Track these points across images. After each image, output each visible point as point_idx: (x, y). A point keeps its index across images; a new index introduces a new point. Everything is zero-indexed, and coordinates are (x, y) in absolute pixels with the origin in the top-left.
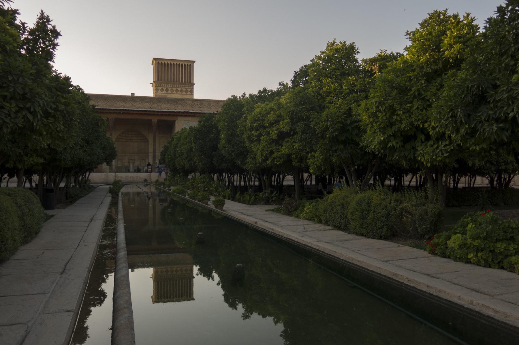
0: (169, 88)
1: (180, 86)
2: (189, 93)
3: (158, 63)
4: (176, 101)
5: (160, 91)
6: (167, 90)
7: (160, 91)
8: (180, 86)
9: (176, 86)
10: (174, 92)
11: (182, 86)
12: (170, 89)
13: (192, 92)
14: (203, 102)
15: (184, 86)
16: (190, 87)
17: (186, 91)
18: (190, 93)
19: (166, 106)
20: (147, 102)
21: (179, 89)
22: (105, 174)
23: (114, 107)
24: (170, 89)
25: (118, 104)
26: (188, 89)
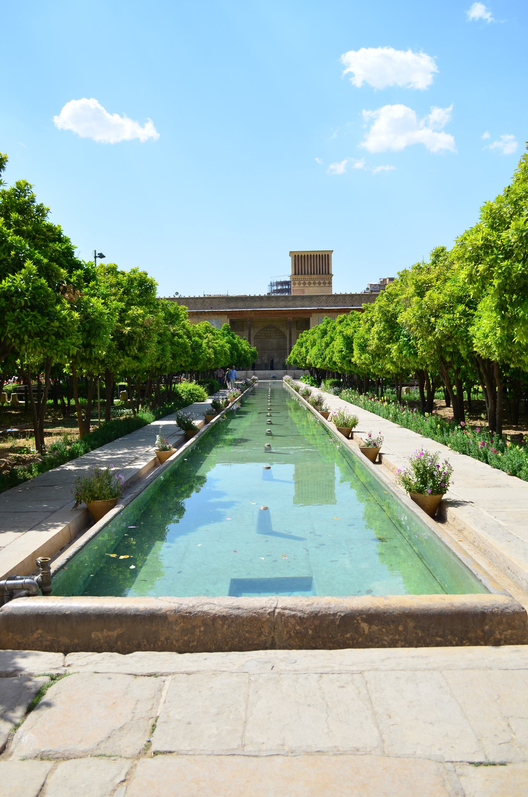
0: (306, 281)
1: (318, 278)
2: (327, 285)
3: (295, 256)
4: (310, 298)
5: (297, 285)
6: (304, 284)
7: (297, 285)
8: (318, 278)
9: (314, 278)
10: (312, 285)
11: (320, 278)
12: (307, 282)
13: (330, 283)
14: (338, 297)
15: (322, 278)
16: (328, 278)
17: (324, 283)
18: (328, 285)
19: (301, 304)
20: (282, 301)
21: (317, 282)
22: (245, 371)
23: (252, 308)
24: (307, 282)
25: (255, 305)
26: (326, 281)
